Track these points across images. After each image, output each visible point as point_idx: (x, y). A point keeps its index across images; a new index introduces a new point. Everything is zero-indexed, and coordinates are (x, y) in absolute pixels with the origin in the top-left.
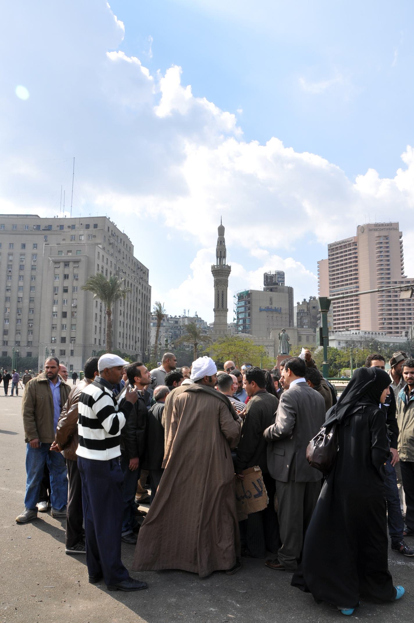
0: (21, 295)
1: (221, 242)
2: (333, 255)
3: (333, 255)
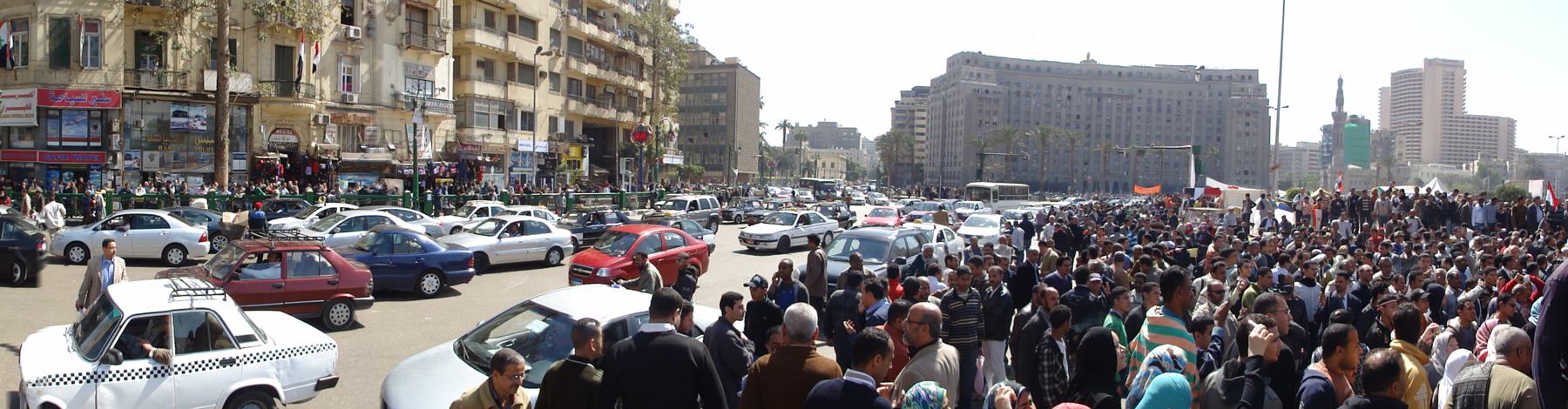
0: (1188, 134)
1: (1340, 92)
2: (1397, 84)
3: (1397, 84)
